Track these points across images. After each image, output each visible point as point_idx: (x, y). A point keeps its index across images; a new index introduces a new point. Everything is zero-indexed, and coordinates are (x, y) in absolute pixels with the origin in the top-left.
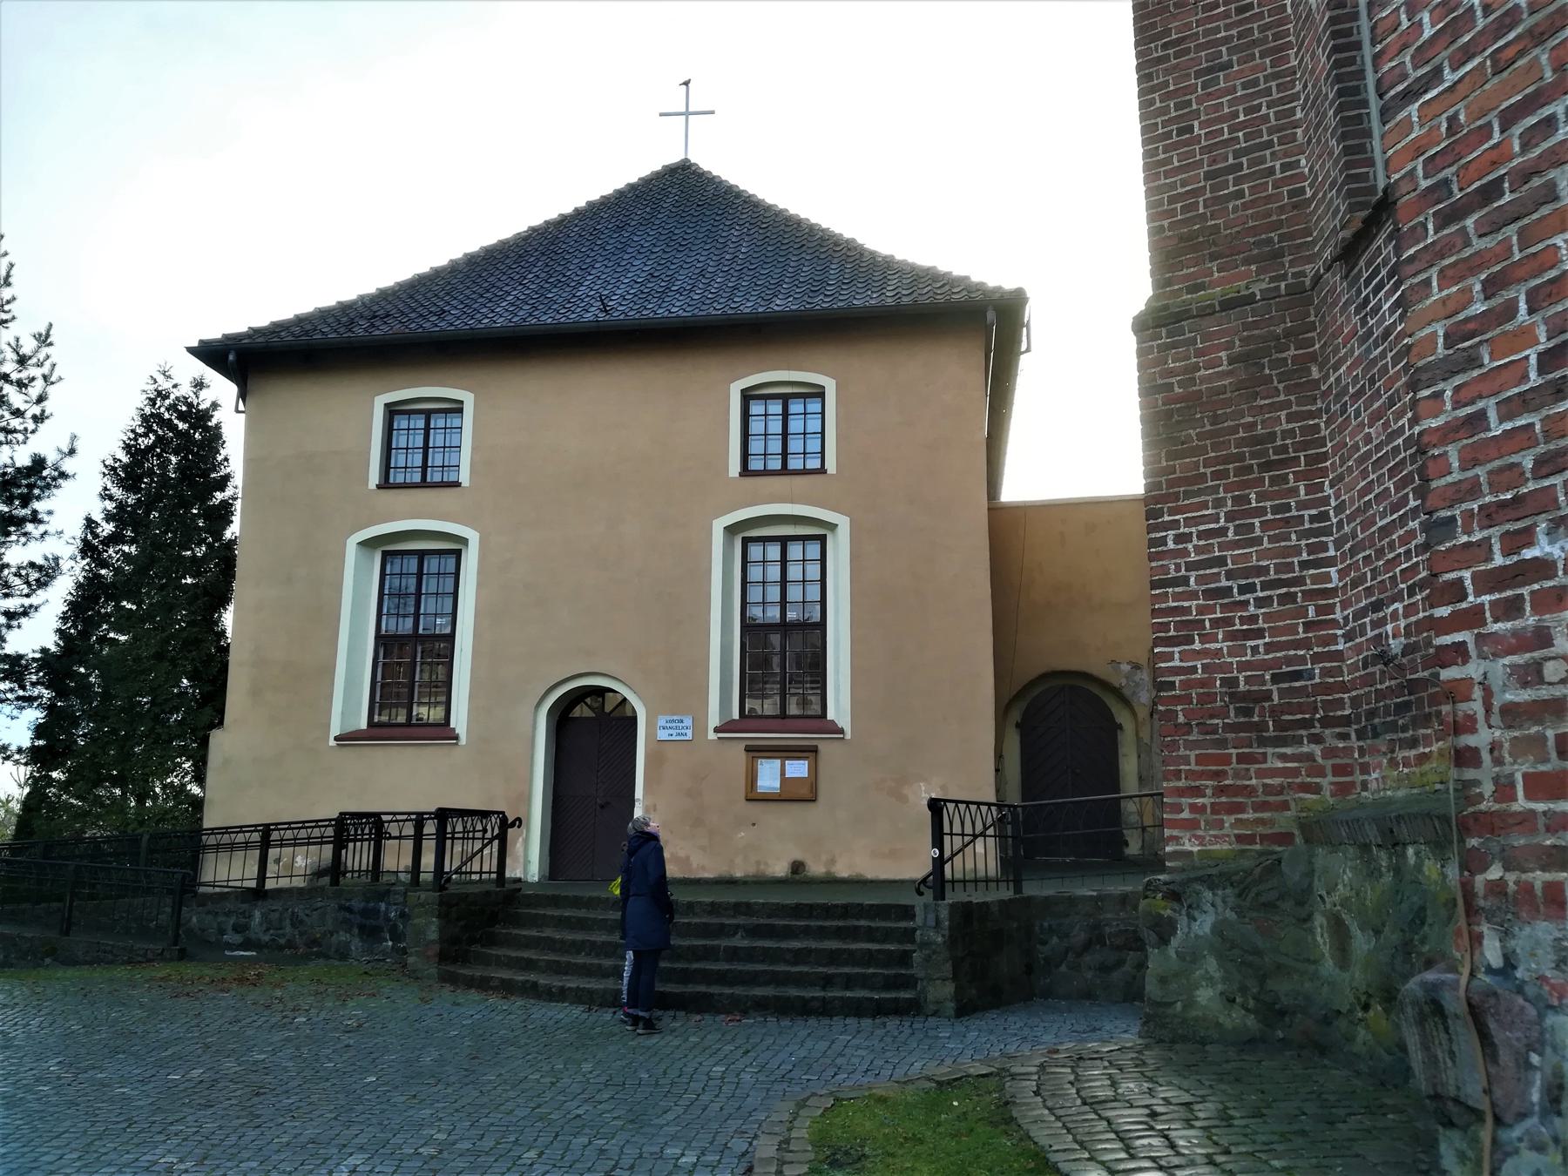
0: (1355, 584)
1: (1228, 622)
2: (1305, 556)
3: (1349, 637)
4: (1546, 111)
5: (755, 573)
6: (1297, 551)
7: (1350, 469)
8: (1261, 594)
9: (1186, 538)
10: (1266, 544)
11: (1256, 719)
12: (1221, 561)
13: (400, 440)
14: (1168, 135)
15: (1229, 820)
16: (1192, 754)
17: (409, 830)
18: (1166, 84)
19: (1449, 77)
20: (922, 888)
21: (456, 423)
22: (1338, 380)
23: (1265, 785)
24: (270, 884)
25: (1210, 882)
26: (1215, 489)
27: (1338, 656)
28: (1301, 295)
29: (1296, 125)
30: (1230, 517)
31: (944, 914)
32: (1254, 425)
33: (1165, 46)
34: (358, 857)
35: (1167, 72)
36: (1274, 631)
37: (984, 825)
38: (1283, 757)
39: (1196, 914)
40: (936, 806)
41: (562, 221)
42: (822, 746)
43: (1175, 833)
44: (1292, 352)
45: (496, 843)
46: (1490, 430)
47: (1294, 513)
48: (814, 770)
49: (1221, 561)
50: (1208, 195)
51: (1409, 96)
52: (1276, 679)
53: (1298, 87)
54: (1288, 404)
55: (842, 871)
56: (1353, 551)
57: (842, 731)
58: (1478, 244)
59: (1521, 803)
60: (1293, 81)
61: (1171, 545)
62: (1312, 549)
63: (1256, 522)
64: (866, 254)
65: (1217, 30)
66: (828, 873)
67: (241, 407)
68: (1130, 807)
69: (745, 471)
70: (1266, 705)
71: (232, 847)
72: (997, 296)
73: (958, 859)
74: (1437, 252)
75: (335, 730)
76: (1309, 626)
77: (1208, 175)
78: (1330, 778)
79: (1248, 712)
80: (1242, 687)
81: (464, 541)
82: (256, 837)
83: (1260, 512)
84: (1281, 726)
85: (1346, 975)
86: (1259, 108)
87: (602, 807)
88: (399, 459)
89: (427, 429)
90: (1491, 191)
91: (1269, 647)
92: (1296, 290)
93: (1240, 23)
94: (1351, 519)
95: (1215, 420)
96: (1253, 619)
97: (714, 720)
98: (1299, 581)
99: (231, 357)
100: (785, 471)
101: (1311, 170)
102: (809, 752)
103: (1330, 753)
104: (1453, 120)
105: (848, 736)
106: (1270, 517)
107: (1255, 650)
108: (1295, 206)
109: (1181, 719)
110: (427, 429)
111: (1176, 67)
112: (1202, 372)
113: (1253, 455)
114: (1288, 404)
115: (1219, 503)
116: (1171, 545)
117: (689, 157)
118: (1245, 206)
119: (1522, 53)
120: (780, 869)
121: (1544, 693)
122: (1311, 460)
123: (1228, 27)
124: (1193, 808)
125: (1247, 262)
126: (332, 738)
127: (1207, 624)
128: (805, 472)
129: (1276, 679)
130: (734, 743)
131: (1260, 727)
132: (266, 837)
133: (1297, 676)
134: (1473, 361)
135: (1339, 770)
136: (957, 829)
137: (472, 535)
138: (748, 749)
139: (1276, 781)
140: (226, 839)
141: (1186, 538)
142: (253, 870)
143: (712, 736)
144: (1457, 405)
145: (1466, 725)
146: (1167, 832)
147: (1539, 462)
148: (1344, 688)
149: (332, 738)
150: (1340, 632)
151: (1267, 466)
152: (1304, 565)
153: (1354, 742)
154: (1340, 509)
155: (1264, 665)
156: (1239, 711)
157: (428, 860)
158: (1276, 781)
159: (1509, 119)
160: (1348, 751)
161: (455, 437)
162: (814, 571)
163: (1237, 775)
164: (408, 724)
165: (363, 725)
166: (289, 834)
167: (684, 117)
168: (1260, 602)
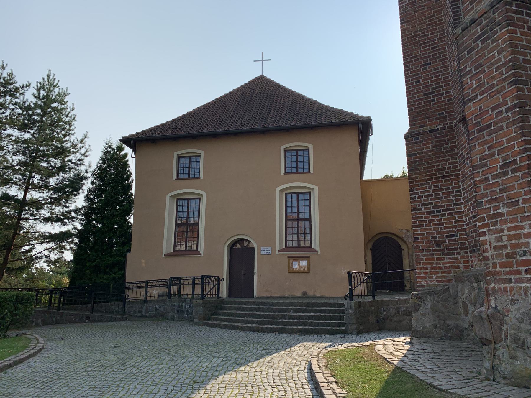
0: (468, 210)
1: (433, 221)
2: (454, 202)
3: (467, 225)
4: (501, 109)
5: (289, 204)
6: (452, 201)
8: (442, 213)
10: (443, 199)
11: (442, 248)
12: (431, 204)
13: (181, 165)
14: (413, 83)
15: (435, 276)
16: (424, 258)
17: (191, 282)
18: (412, 69)
19: (480, 97)
20: (346, 298)
21: (198, 160)
22: (462, 153)
23: (444, 266)
24: (148, 299)
25: (430, 294)
26: (429, 183)
27: (464, 230)
29: (449, 81)
30: (433, 191)
31: (353, 305)
32: (440, 165)
33: (412, 58)
34: (174, 290)
35: (412, 65)
37: (364, 279)
38: (449, 258)
39: (425, 302)
40: (349, 273)
41: (226, 96)
42: (311, 256)
43: (420, 280)
44: (450, 145)
45: (217, 286)
46: (489, 182)
47: (451, 190)
48: (309, 264)
49: (431, 204)
50: (425, 100)
51: (470, 100)
52: (447, 237)
53: (450, 71)
54: (448, 160)
55: (318, 295)
56: (468, 201)
57: (317, 251)
58: (486, 138)
59: (498, 269)
60: (448, 69)
61: (417, 199)
62: (456, 200)
63: (441, 192)
64: (320, 105)
65: (426, 54)
66: (314, 295)
67: (134, 156)
68: (406, 275)
69: (286, 173)
70: (444, 244)
71: (137, 287)
72: (362, 119)
73: (356, 289)
74: (478, 138)
75: (164, 252)
76: (456, 222)
77: (425, 95)
78: (463, 264)
79: (439, 246)
80: (438, 239)
81: (202, 195)
82: (144, 284)
83: (442, 190)
84: (449, 250)
85: (467, 318)
86: (438, 76)
87: (244, 275)
88: (181, 171)
89: (190, 162)
90: (489, 126)
91: (445, 228)
92: (450, 127)
93: (433, 52)
94: (467, 192)
95: (428, 164)
96: (440, 220)
97: (278, 248)
98: (453, 209)
99: (132, 142)
100: (297, 172)
101: (454, 94)
102: (307, 258)
103: (463, 257)
104: (481, 107)
105: (319, 253)
106: (444, 191)
107: (441, 228)
108: (449, 104)
109: (421, 248)
110: (190, 162)
111: (415, 64)
112: (424, 150)
114: (448, 160)
115: (430, 187)
116: (417, 199)
117: (263, 74)
118: (435, 104)
119: (495, 95)
120: (299, 294)
121: (502, 243)
122: (455, 175)
124: (424, 273)
125: (436, 119)
126: (163, 255)
127: (428, 221)
128: (304, 173)
129: (447, 237)
131: (444, 250)
132: (147, 285)
133: (453, 236)
134: (486, 165)
135: (465, 262)
136: (356, 280)
137: (204, 194)
138: (289, 257)
139: (448, 265)
140: (135, 285)
142: (143, 294)
143: (277, 253)
144: (483, 175)
145: (486, 251)
146: (417, 280)
147: (501, 190)
149: (163, 255)
150: (465, 224)
151: (443, 177)
152: (454, 205)
153: (469, 254)
154: (464, 189)
155: (443, 233)
156: (437, 246)
157: (198, 292)
158: (448, 265)
159: (493, 109)
160: (467, 257)
161: (198, 164)
162: (307, 203)
163: (437, 263)
164: (186, 250)
165: (172, 251)
166: (153, 284)
168: (442, 215)
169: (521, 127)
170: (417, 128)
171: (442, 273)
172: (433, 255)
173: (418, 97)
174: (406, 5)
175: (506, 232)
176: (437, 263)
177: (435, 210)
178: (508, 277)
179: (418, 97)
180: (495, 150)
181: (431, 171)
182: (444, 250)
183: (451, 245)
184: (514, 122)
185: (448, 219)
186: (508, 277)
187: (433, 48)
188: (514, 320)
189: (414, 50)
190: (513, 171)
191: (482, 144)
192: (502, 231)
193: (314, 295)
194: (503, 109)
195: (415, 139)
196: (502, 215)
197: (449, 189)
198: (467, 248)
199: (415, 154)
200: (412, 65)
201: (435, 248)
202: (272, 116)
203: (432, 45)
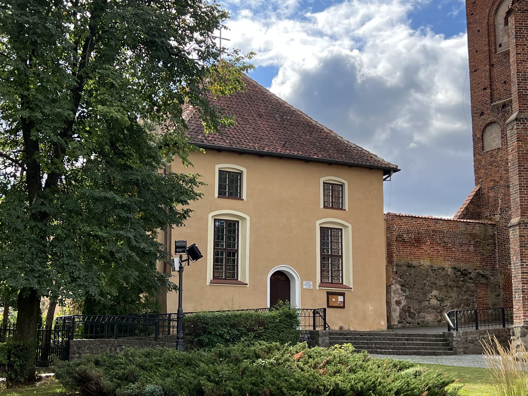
33: (524, 168)
61: (525, 266)
69: (325, 207)
102: (343, 294)
130: (323, 290)
143: (318, 288)
167: (222, 40)
174: (521, 128)
193: (349, 329)
200: (524, 174)
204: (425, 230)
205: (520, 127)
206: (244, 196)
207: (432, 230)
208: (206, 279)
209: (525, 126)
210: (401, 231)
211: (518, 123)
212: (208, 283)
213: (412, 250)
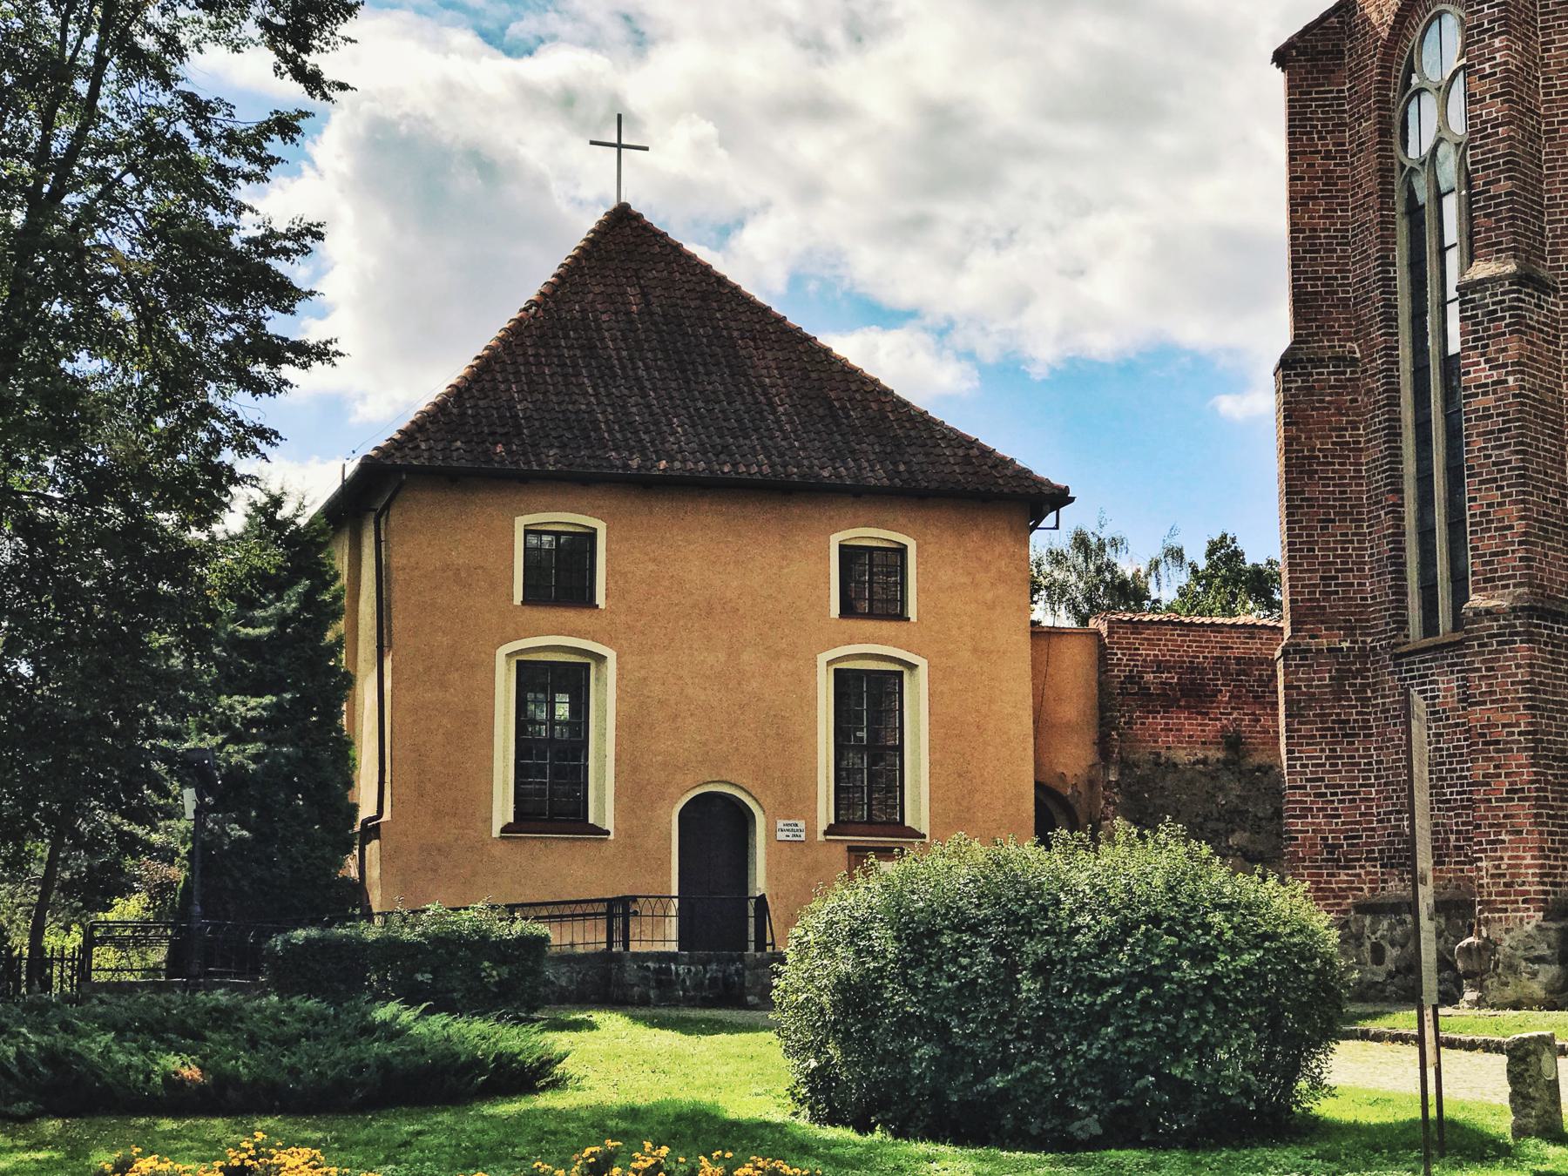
3: (1379, 821)
6: (1357, 778)
7: (1388, 748)
9: (1306, 766)
12: (1322, 779)
14: (1301, 550)
15: (1322, 903)
19: (1489, 706)
22: (1384, 704)
26: (1321, 743)
27: (1373, 829)
28: (1363, 654)
29: (1365, 563)
30: (1327, 758)
33: (1302, 500)
35: (1303, 514)
36: (1346, 816)
49: (1322, 779)
52: (1345, 839)
54: (1356, 707)
56: (1386, 784)
58: (1492, 754)
59: (1493, 898)
62: (1364, 778)
65: (1328, 499)
74: (1482, 751)
76: (1361, 815)
80: (1330, 842)
83: (1341, 757)
84: (1347, 860)
86: (1347, 549)
90: (1497, 742)
91: (1344, 823)
95: (1322, 708)
96: (1337, 809)
97: (822, 826)
98: (1358, 793)
103: (1368, 873)
107: (1337, 824)
108: (1363, 606)
113: (1340, 729)
114: (1356, 707)
123: (1335, 500)
125: (1340, 628)
129: (1346, 838)
131: (1339, 860)
135: (1371, 881)
137: (610, 654)
138: (850, 849)
141: (1306, 766)
143: (821, 837)
148: (1376, 844)
152: (1360, 786)
153: (1378, 869)
154: (1379, 762)
156: (1328, 853)
159: (1504, 726)
160: (1376, 873)
163: (1326, 882)
168: (1341, 801)
169: (1533, 757)
170: (1303, 638)
171: (1335, 898)
172: (1320, 867)
173: (1310, 579)
174: (1297, 388)
175: (1506, 861)
176: (1326, 882)
177: (1328, 791)
178: (1504, 906)
179: (1310, 579)
180: (1503, 772)
181: (1326, 722)
182: (1339, 860)
183: (1350, 853)
184: (1526, 749)
185: (1349, 809)
186: (1504, 906)
187: (1341, 492)
188: (1508, 949)
189: (1307, 485)
190: (1520, 799)
191: (1485, 759)
192: (1501, 858)
194: (1516, 730)
195: (1301, 659)
196: (1503, 842)
197: (1354, 757)
198: (1375, 859)
199: (1299, 687)
200: (1303, 514)
201: (1325, 856)
202: (781, 430)
203: (1346, 499)
204: (1213, 658)
205: (1293, 385)
206: (600, 599)
207: (1235, 658)
208: (488, 820)
209: (1308, 381)
210: (1136, 666)
211: (1289, 375)
212: (496, 833)
213: (1172, 718)
